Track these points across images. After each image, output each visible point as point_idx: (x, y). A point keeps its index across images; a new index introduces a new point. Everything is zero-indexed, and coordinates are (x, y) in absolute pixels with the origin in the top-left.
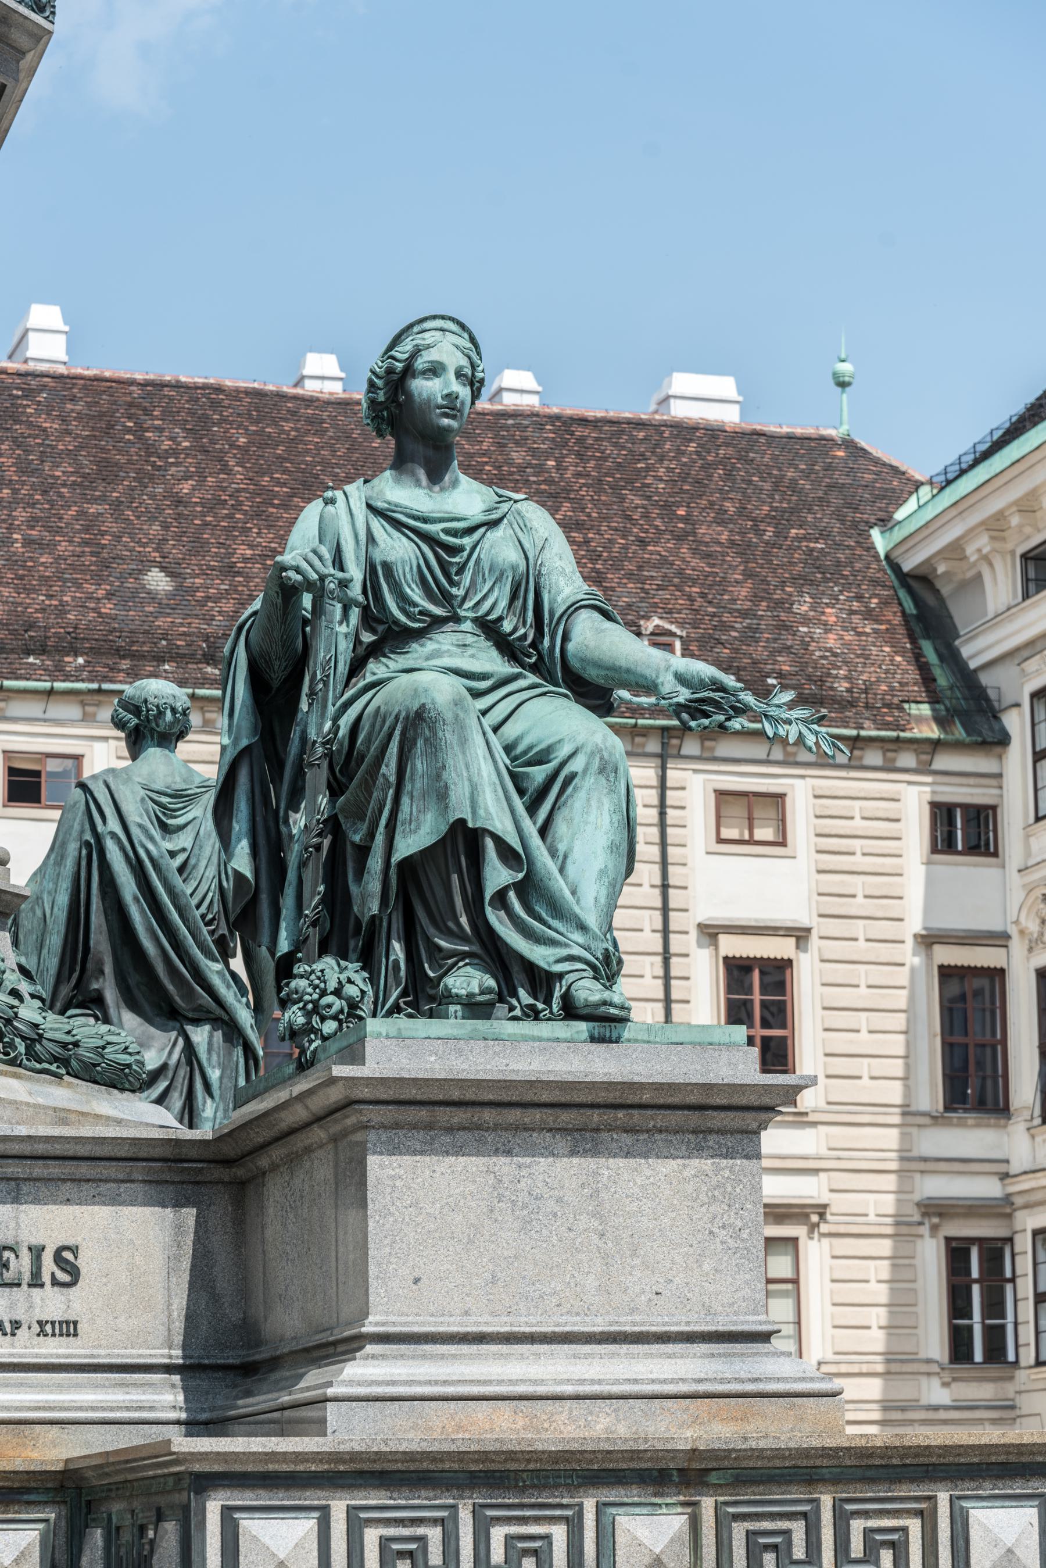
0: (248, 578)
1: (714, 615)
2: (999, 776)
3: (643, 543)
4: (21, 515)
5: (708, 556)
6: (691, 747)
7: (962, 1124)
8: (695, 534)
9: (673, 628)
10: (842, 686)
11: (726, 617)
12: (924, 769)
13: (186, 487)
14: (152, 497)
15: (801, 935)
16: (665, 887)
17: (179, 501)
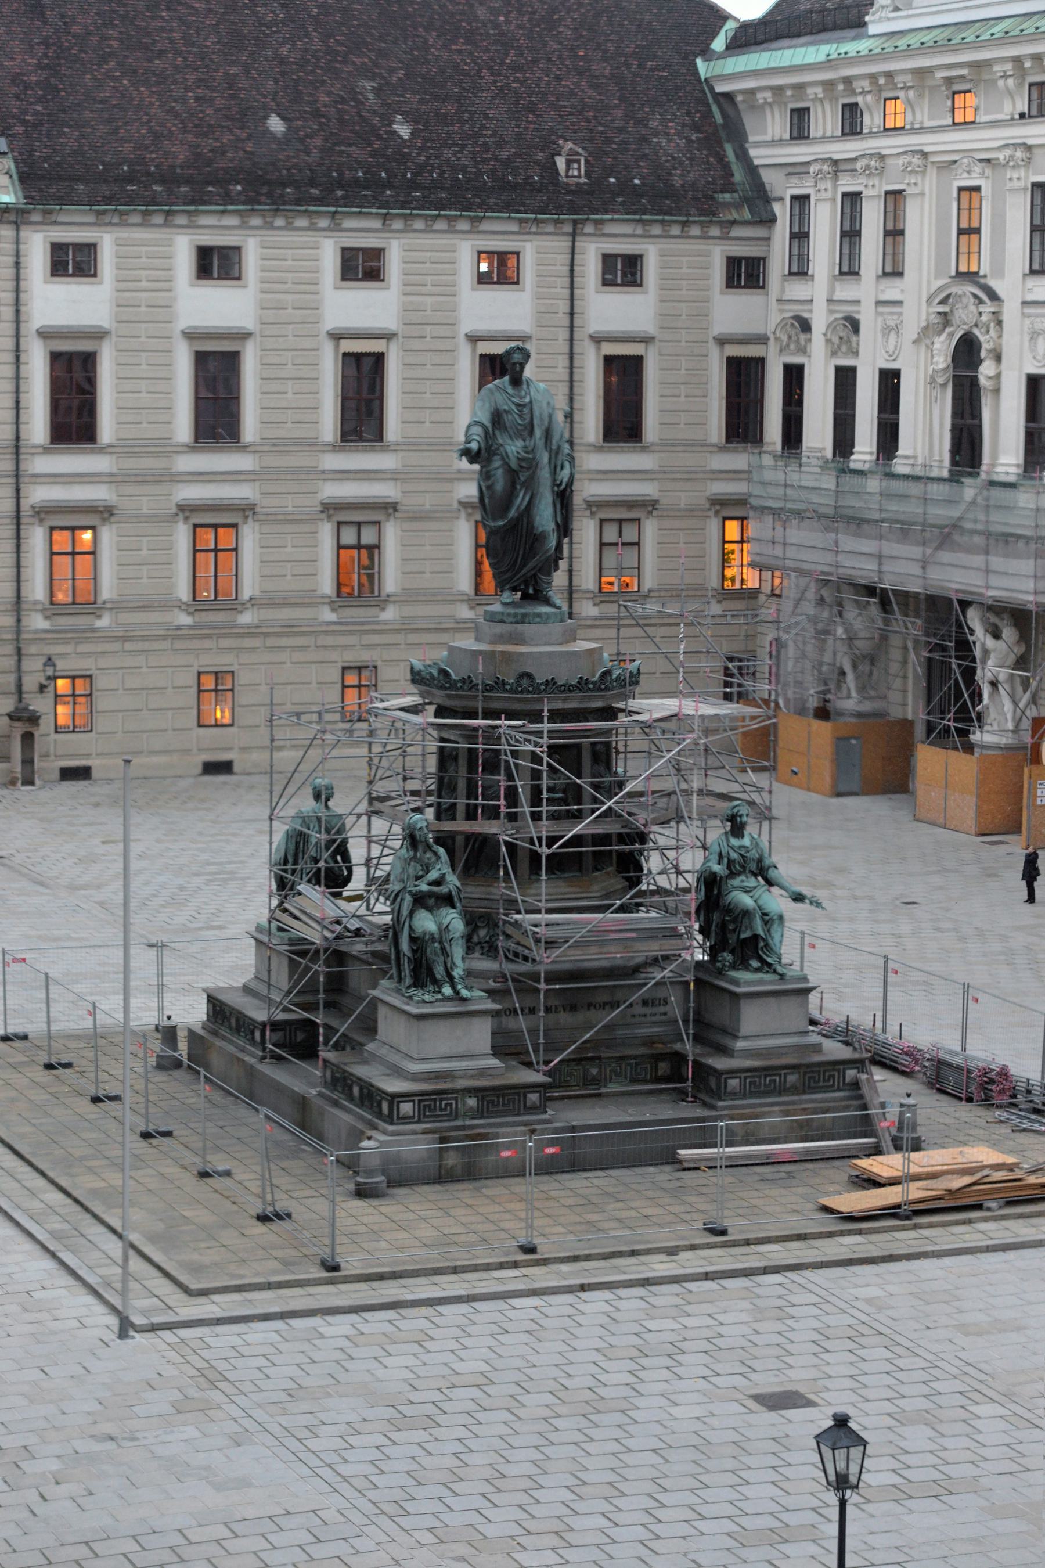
0: (329, 120)
1: (602, 132)
2: (768, 239)
3: (558, 79)
4: (191, 77)
5: (598, 86)
6: (589, 229)
7: (735, 450)
8: (590, 70)
9: (580, 150)
10: (677, 181)
11: (610, 134)
12: (725, 237)
13: (284, 51)
14: (266, 59)
15: (647, 340)
16: (572, 314)
17: (282, 61)
